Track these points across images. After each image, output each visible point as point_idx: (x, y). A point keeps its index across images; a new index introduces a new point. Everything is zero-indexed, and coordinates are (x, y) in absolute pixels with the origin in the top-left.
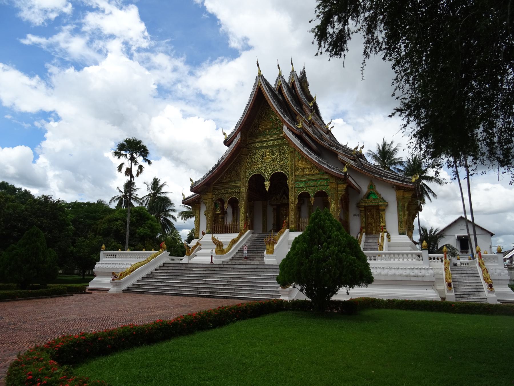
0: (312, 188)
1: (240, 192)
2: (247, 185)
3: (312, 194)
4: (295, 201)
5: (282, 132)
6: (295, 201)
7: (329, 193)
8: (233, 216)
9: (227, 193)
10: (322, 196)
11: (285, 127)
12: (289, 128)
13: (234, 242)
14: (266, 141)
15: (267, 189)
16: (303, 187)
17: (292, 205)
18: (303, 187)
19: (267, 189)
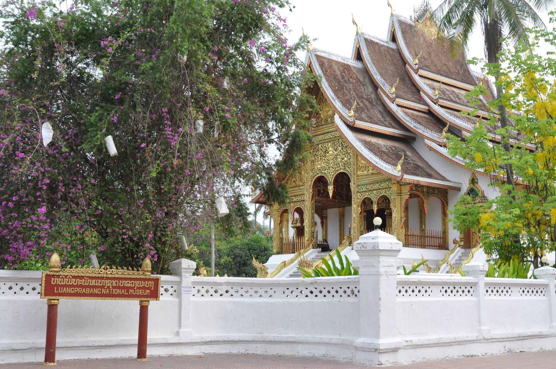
0: (375, 192)
1: (304, 201)
2: (311, 190)
3: (375, 200)
4: (357, 210)
5: (333, 122)
6: (357, 210)
7: (392, 198)
8: (323, 228)
9: (292, 202)
10: (385, 200)
11: (336, 117)
12: (342, 117)
13: (284, 264)
14: (328, 132)
15: (331, 195)
16: (366, 191)
17: (354, 215)
18: (366, 191)
19: (331, 195)
